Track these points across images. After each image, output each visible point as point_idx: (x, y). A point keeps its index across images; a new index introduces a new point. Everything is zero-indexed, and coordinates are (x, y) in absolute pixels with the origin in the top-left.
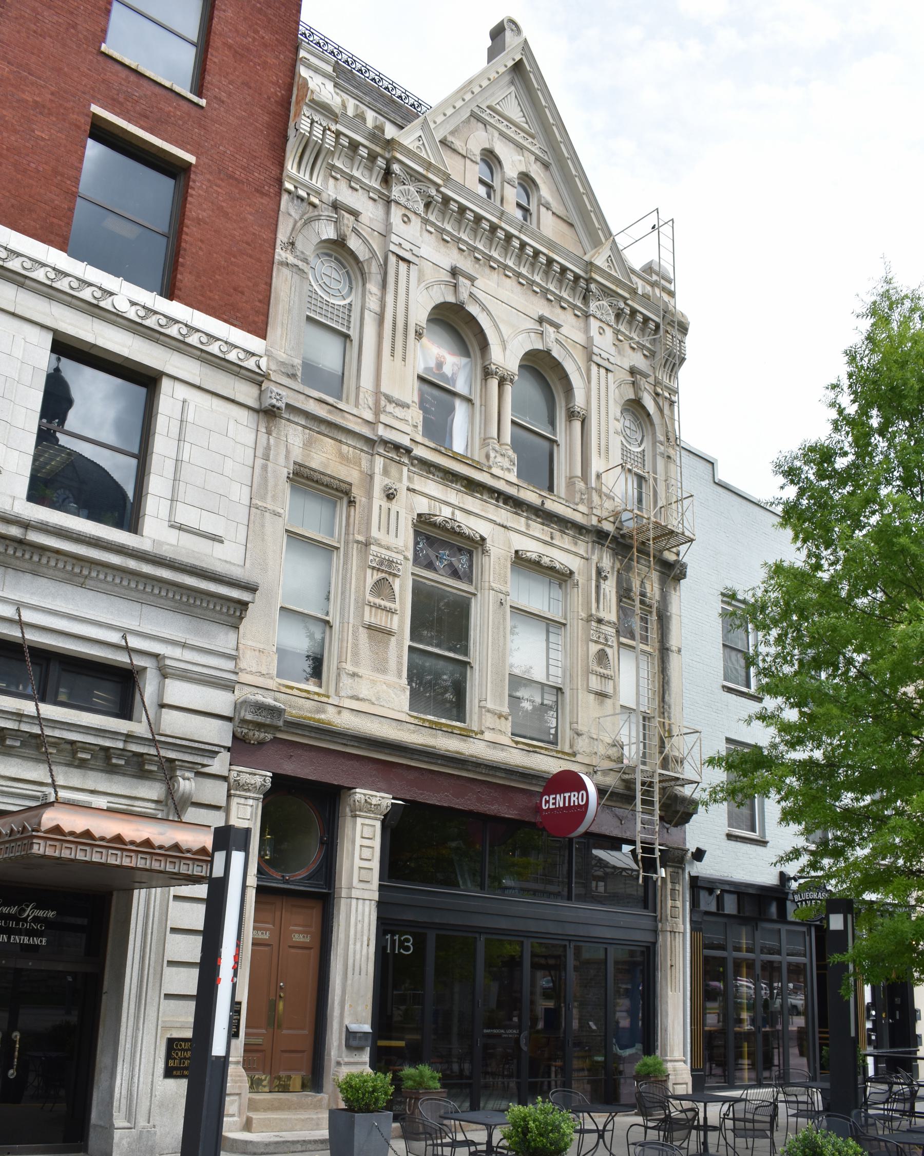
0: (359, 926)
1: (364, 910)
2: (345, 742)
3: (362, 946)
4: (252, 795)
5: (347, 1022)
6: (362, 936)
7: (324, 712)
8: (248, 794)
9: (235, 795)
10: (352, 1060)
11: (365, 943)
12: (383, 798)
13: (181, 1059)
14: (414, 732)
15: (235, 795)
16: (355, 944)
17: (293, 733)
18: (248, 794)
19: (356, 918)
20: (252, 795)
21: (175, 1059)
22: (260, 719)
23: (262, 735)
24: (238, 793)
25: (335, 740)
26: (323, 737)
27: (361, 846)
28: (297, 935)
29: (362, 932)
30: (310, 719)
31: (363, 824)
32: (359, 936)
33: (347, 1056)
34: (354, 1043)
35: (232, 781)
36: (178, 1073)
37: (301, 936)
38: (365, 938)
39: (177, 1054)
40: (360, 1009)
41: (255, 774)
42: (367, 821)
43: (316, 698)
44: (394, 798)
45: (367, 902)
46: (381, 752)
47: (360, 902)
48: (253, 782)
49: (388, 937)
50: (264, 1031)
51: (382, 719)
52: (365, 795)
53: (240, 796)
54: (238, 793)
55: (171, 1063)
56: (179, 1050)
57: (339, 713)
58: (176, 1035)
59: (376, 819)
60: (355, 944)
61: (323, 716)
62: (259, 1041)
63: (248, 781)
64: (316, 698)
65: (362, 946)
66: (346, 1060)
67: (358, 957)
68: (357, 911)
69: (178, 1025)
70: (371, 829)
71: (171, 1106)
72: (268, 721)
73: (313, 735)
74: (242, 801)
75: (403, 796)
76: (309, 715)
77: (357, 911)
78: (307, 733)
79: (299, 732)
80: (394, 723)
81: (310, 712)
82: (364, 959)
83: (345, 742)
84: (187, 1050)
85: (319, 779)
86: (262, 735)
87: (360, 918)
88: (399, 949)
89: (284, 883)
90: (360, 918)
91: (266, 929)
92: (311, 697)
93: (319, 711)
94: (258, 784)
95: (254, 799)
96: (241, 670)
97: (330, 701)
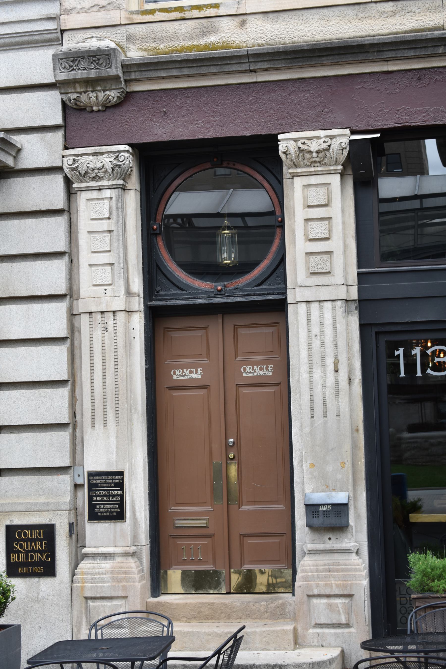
0: (316, 343)
1: (322, 318)
2: (245, 67)
3: (324, 372)
4: (105, 183)
5: (308, 490)
6: (323, 357)
7: (214, 30)
8: (100, 183)
9: (81, 190)
10: (321, 546)
11: (331, 368)
12: (332, 137)
13: (27, 552)
14: (394, 14)
15: (81, 190)
16: (310, 371)
17: (158, 78)
18: (100, 183)
19: (309, 332)
20: (105, 183)
21: (18, 552)
22: (79, 74)
23: (101, 95)
24: (84, 185)
25: (227, 68)
26: (204, 70)
27: (307, 220)
28: (249, 369)
29: (323, 352)
30: (190, 49)
31: (306, 186)
32: (316, 358)
33: (313, 541)
34: (316, 522)
35: (66, 170)
36: (26, 570)
37: (257, 369)
38: (330, 361)
39: (21, 546)
40: (330, 468)
41: (102, 154)
42: (313, 180)
43: (196, 13)
44: (353, 132)
45: (328, 305)
46: (322, 65)
47: (315, 306)
48: (99, 165)
49: (400, 352)
50: (209, 508)
51: (325, 11)
52: (296, 140)
53: (88, 189)
54: (84, 185)
55: (14, 558)
56: (23, 540)
57: (243, 24)
58: (18, 521)
59: (329, 173)
60: (310, 371)
61: (213, 39)
62: (202, 522)
63: (91, 166)
64: (196, 13)
65: (324, 372)
66: (310, 546)
67: (318, 390)
68: (309, 321)
69: (22, 508)
70: (323, 190)
71: (21, 612)
72: (93, 74)
73: (186, 72)
74: (94, 194)
75: (380, 125)
76: (189, 43)
77: (309, 321)
78: (175, 73)
79: (162, 74)
80: (350, 11)
81: (190, 39)
82: (330, 392)
83: (245, 67)
84: (35, 540)
85: (218, 135)
86: (101, 95)
87: (315, 330)
88: (424, 370)
89: (216, 296)
90: (315, 330)
91: (196, 367)
92: (187, 15)
93: (204, 33)
94: (108, 166)
95: (110, 188)
96: (68, 12)
97: (221, 11)
